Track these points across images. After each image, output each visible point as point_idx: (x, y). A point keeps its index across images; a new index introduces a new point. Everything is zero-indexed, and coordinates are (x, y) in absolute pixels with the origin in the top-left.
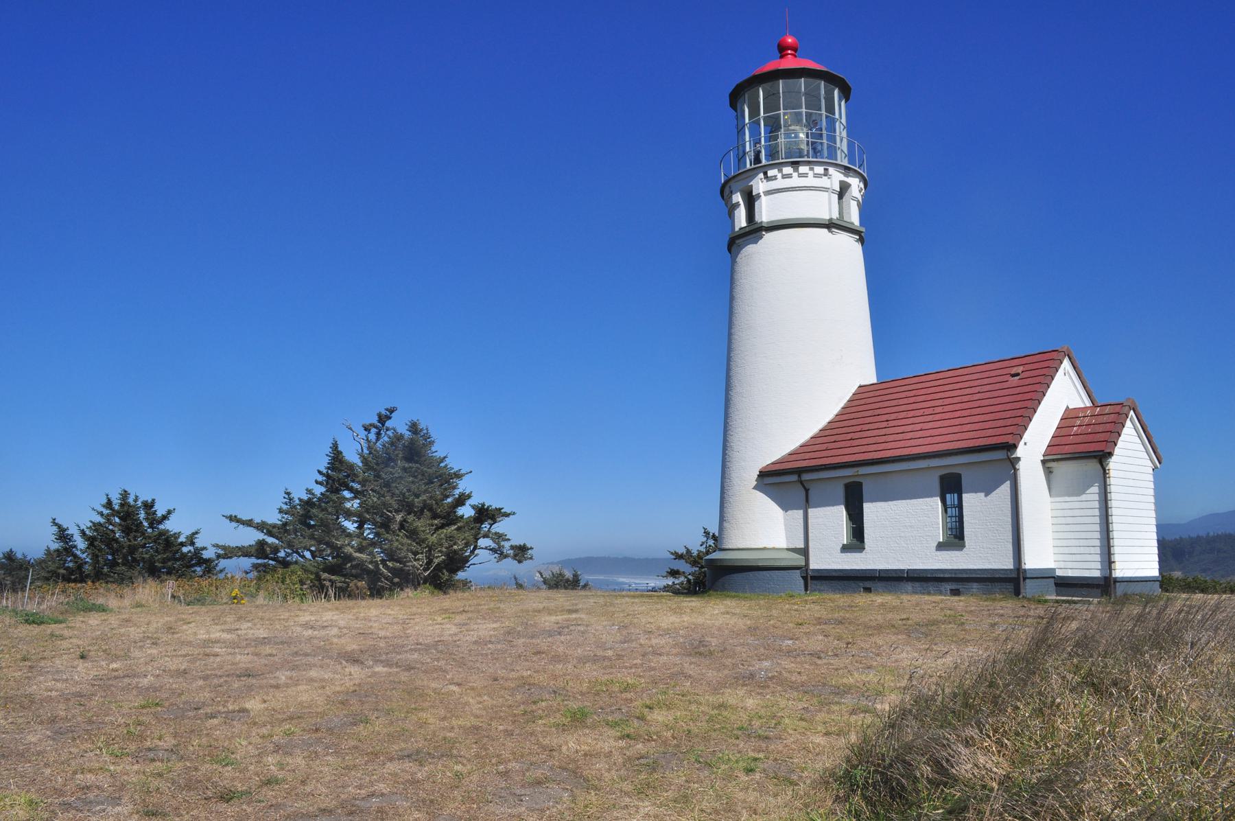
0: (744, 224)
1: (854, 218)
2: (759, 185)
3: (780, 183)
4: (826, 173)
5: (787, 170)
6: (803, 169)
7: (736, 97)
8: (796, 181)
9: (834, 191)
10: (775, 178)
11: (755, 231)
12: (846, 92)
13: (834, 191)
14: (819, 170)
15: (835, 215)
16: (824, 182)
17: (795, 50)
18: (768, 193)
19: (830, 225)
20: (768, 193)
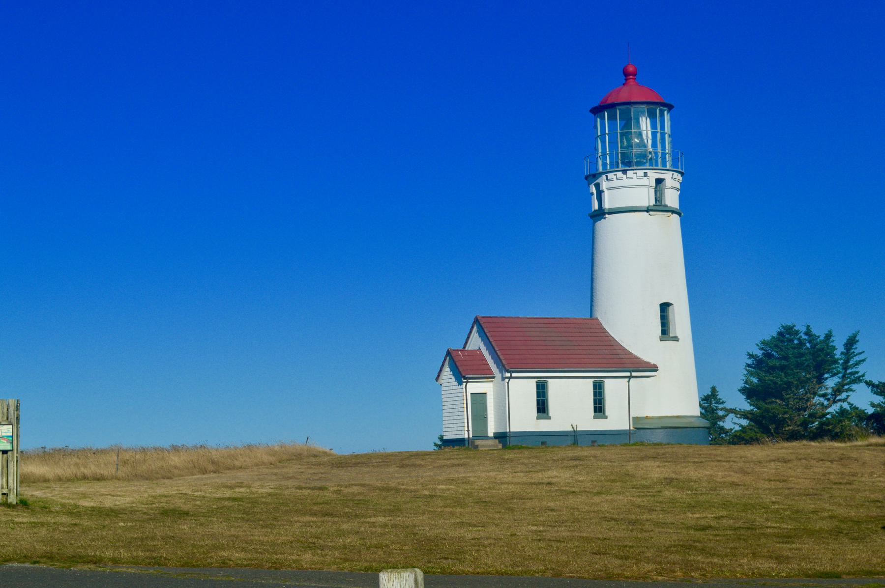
0: (596, 207)
1: (672, 198)
2: (604, 185)
3: (615, 183)
4: (646, 175)
5: (620, 174)
6: (630, 173)
7: (597, 111)
8: (625, 182)
9: (649, 187)
10: (612, 180)
11: (600, 214)
12: (670, 107)
13: (649, 187)
14: (641, 173)
15: (652, 202)
16: (645, 181)
17: (635, 74)
18: (609, 189)
19: (648, 210)
20: (609, 189)
